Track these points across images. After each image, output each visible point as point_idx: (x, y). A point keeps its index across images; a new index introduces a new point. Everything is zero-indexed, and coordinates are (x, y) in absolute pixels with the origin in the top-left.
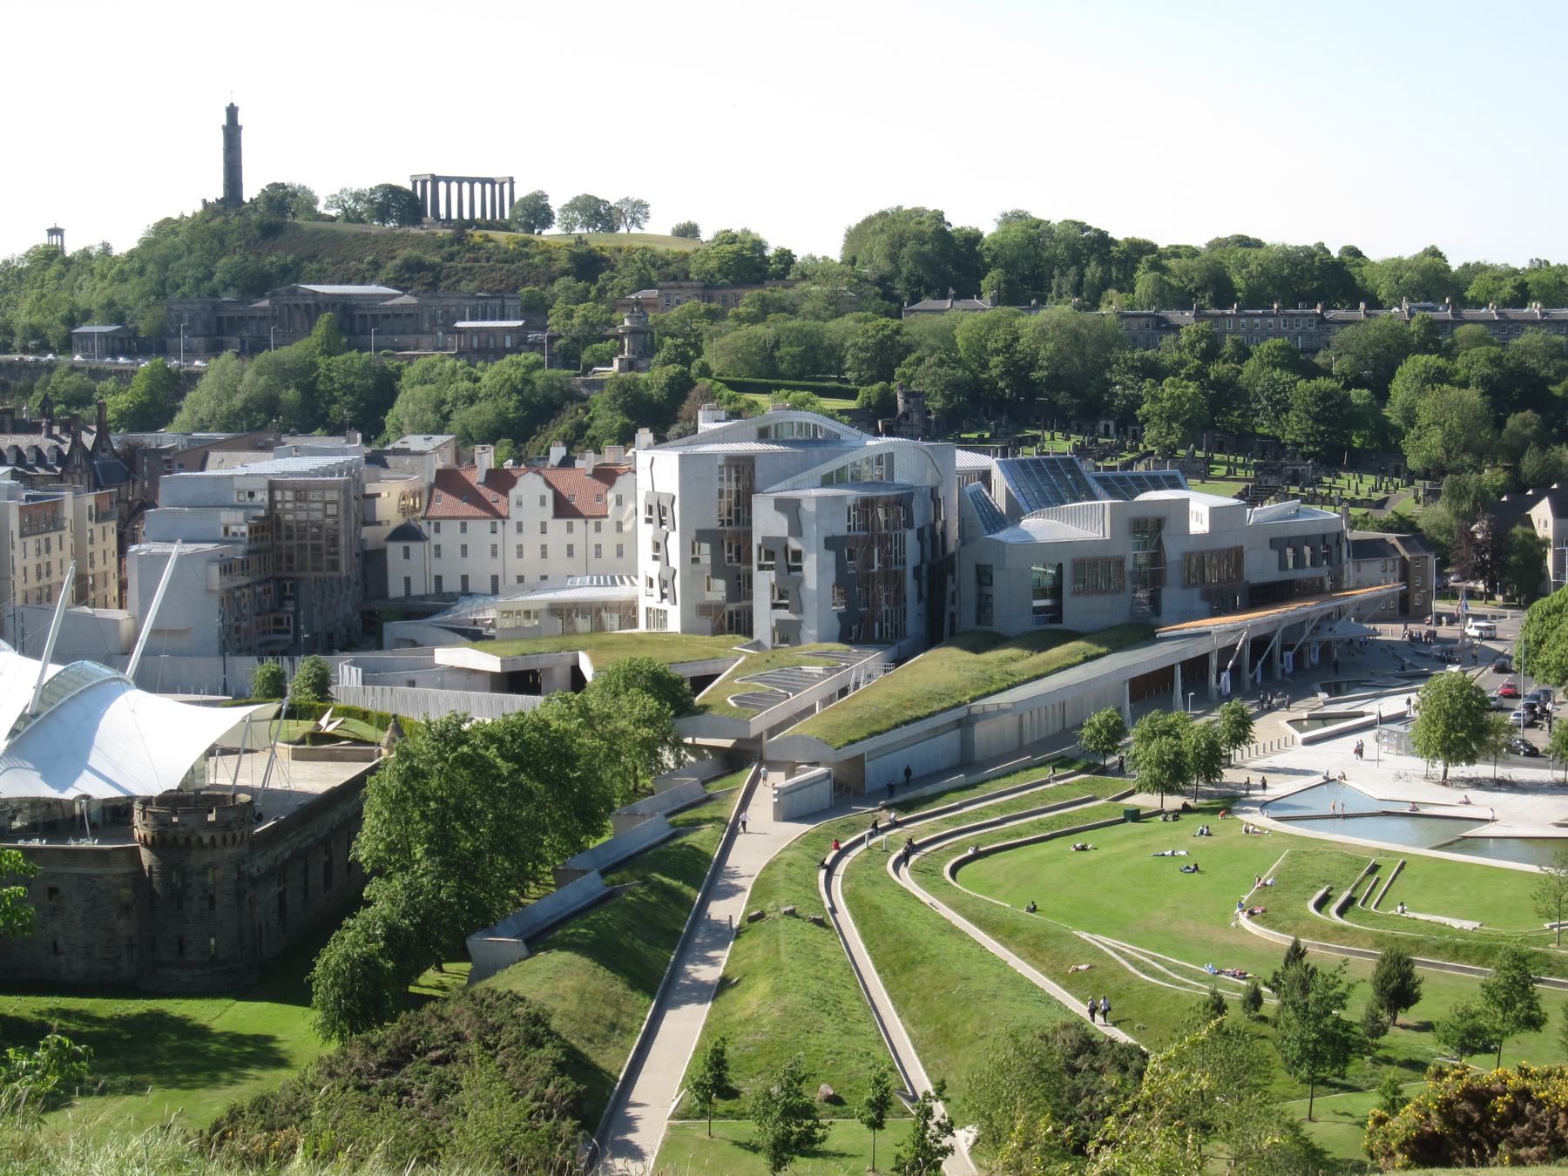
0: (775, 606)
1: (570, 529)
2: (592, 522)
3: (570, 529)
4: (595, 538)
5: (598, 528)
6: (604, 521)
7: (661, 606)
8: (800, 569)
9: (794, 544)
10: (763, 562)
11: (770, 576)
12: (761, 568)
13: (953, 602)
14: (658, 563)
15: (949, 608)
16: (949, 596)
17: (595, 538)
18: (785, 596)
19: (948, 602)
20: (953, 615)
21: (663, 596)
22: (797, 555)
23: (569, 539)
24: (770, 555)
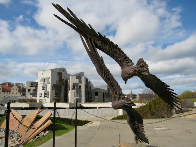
0: (75, 96)
1: (5, 93)
2: (8, 93)
3: (5, 93)
4: (9, 95)
5: (9, 94)
6: (10, 93)
7: (44, 99)
8: (81, 89)
9: (80, 84)
10: (73, 88)
11: (75, 91)
12: (72, 89)
13: (90, 98)
14: (44, 91)
15: (90, 99)
16: (89, 97)
17: (9, 95)
18: (78, 93)
19: (89, 98)
20: (90, 100)
21: (45, 97)
22: (80, 87)
23: (4, 95)
24: (74, 87)
